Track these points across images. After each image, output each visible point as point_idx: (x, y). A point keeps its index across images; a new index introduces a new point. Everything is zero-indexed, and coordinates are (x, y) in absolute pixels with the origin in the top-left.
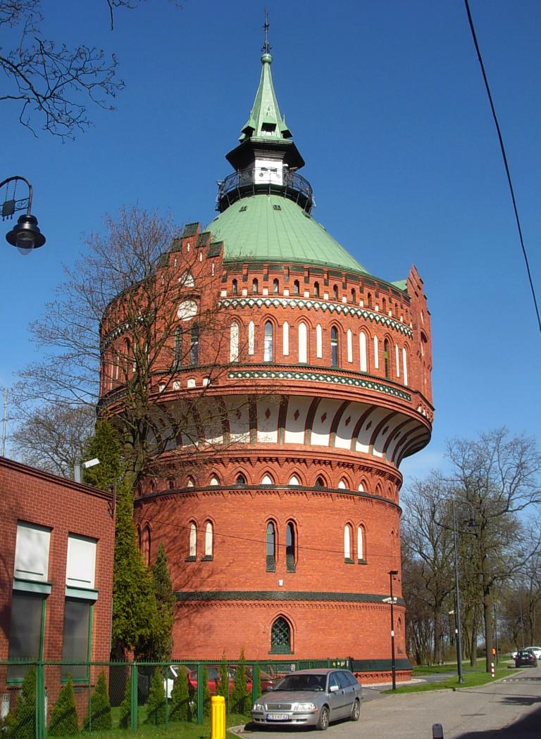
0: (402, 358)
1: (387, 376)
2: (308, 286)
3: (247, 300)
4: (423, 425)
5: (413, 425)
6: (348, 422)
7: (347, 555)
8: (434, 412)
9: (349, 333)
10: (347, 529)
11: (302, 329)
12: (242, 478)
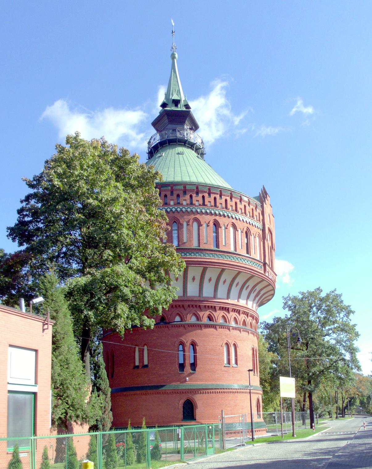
0: (255, 242)
1: (248, 253)
4: (270, 285)
5: (264, 284)
6: (224, 282)
8: (277, 277)
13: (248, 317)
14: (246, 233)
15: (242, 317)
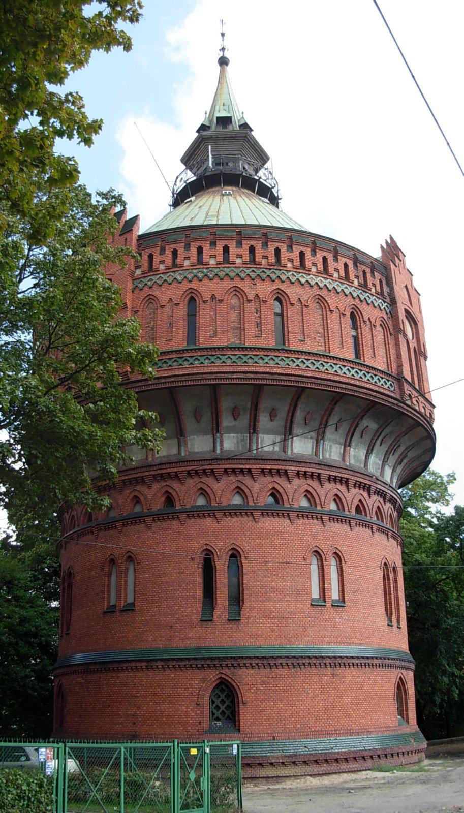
1: (357, 355)
2: (240, 251)
4: (418, 424)
7: (315, 594)
8: (435, 411)
12: (170, 500)
13: (369, 495)
14: (352, 315)
15: (352, 496)
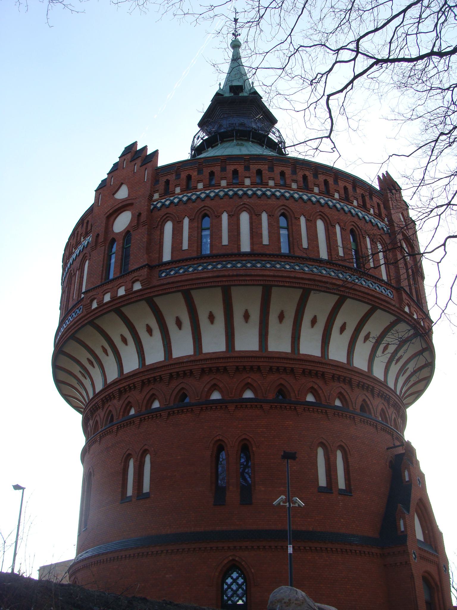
3: (180, 196)
9: (303, 220)
10: (320, 452)
11: (245, 218)
14: (352, 232)
